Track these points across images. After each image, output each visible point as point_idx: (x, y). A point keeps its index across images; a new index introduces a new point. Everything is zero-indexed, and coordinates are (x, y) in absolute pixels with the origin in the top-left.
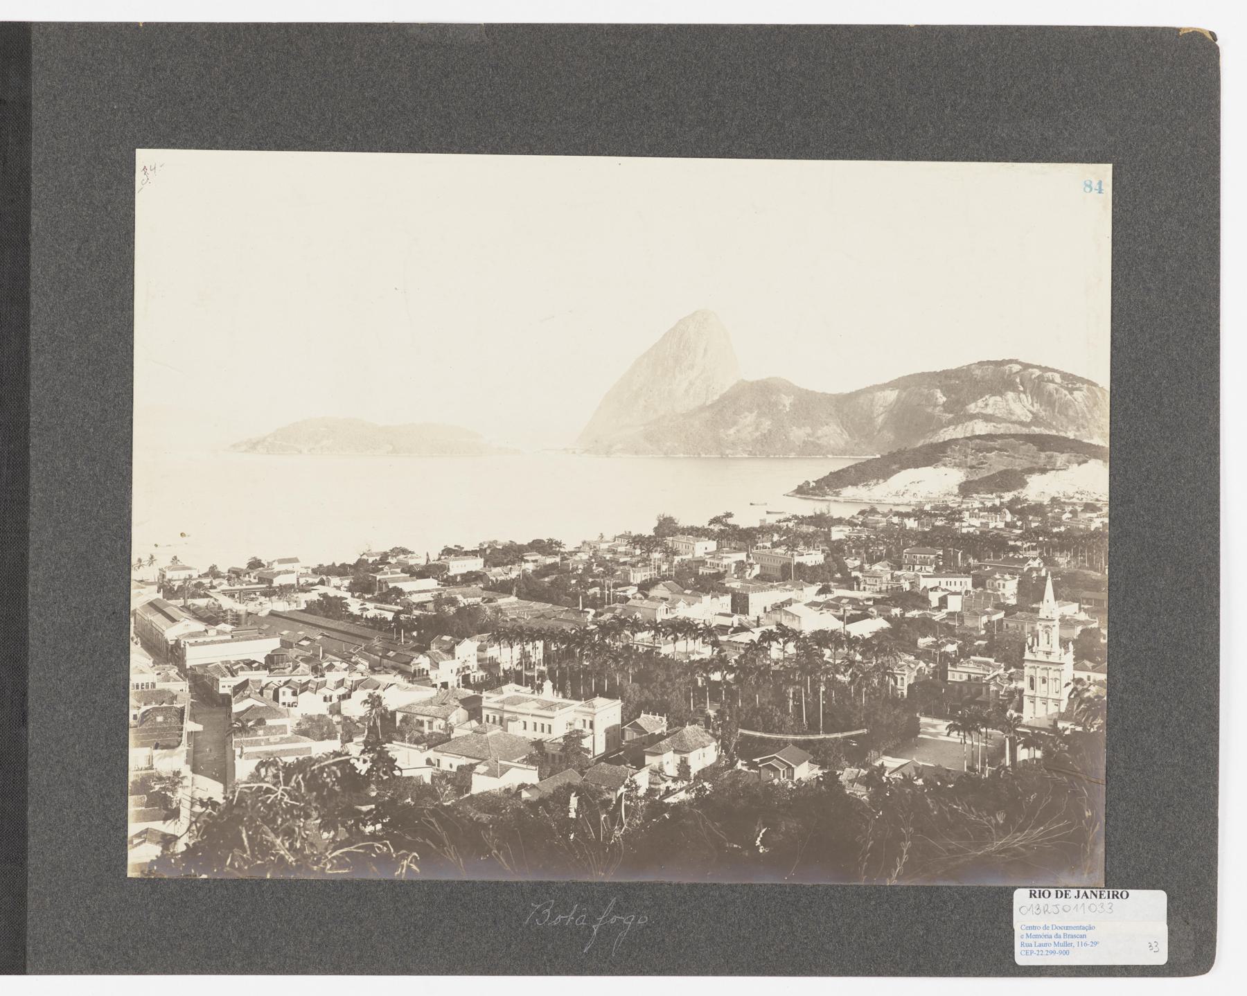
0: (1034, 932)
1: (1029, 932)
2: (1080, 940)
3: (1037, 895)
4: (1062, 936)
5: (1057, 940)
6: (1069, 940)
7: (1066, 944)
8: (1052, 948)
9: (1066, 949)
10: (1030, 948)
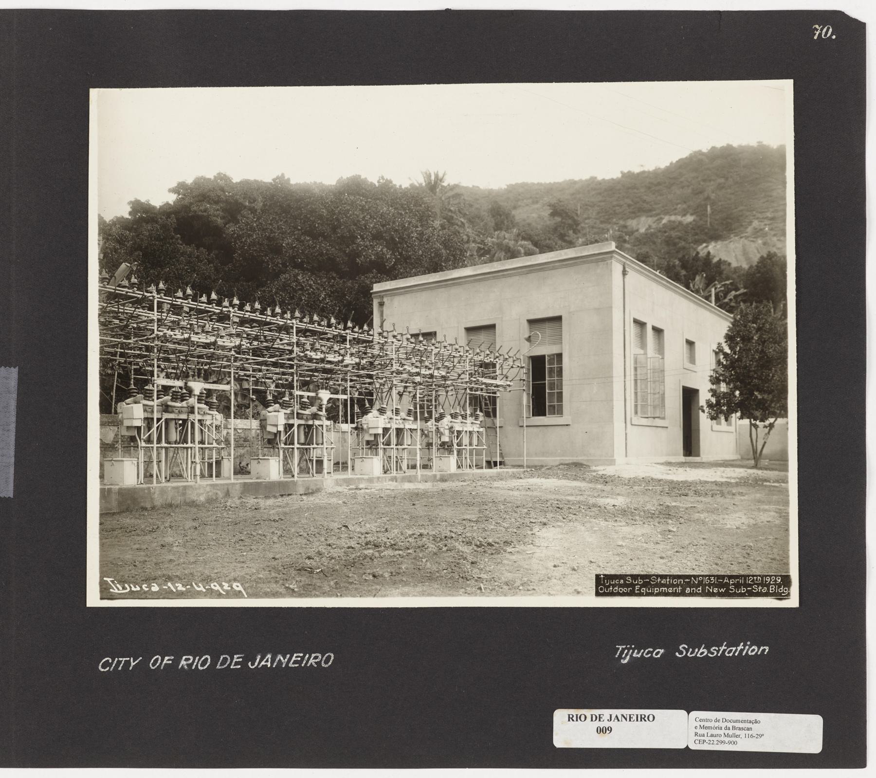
0: (707, 724)
1: (702, 724)
2: (747, 732)
4: (731, 728)
5: (727, 732)
6: (738, 732)
8: (722, 738)
9: (734, 739)
10: (702, 738)
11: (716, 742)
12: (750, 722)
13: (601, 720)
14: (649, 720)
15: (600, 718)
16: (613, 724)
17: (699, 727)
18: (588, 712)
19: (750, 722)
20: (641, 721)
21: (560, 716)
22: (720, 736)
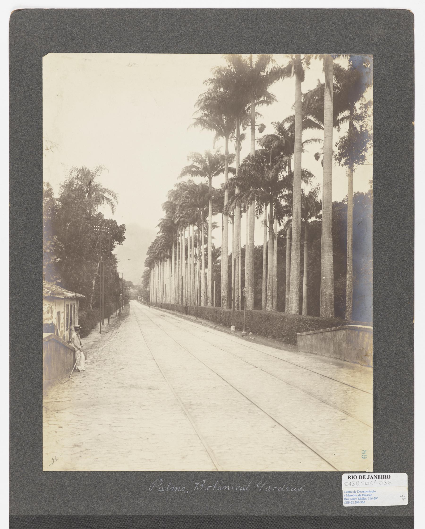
0: (350, 494)
1: (348, 494)
2: (370, 497)
3: (351, 478)
4: (362, 495)
5: (359, 497)
6: (365, 497)
7: (363, 499)
8: (358, 500)
9: (363, 500)
11: (354, 502)
12: (371, 492)
17: (346, 496)
19: (371, 492)
22: (356, 499)
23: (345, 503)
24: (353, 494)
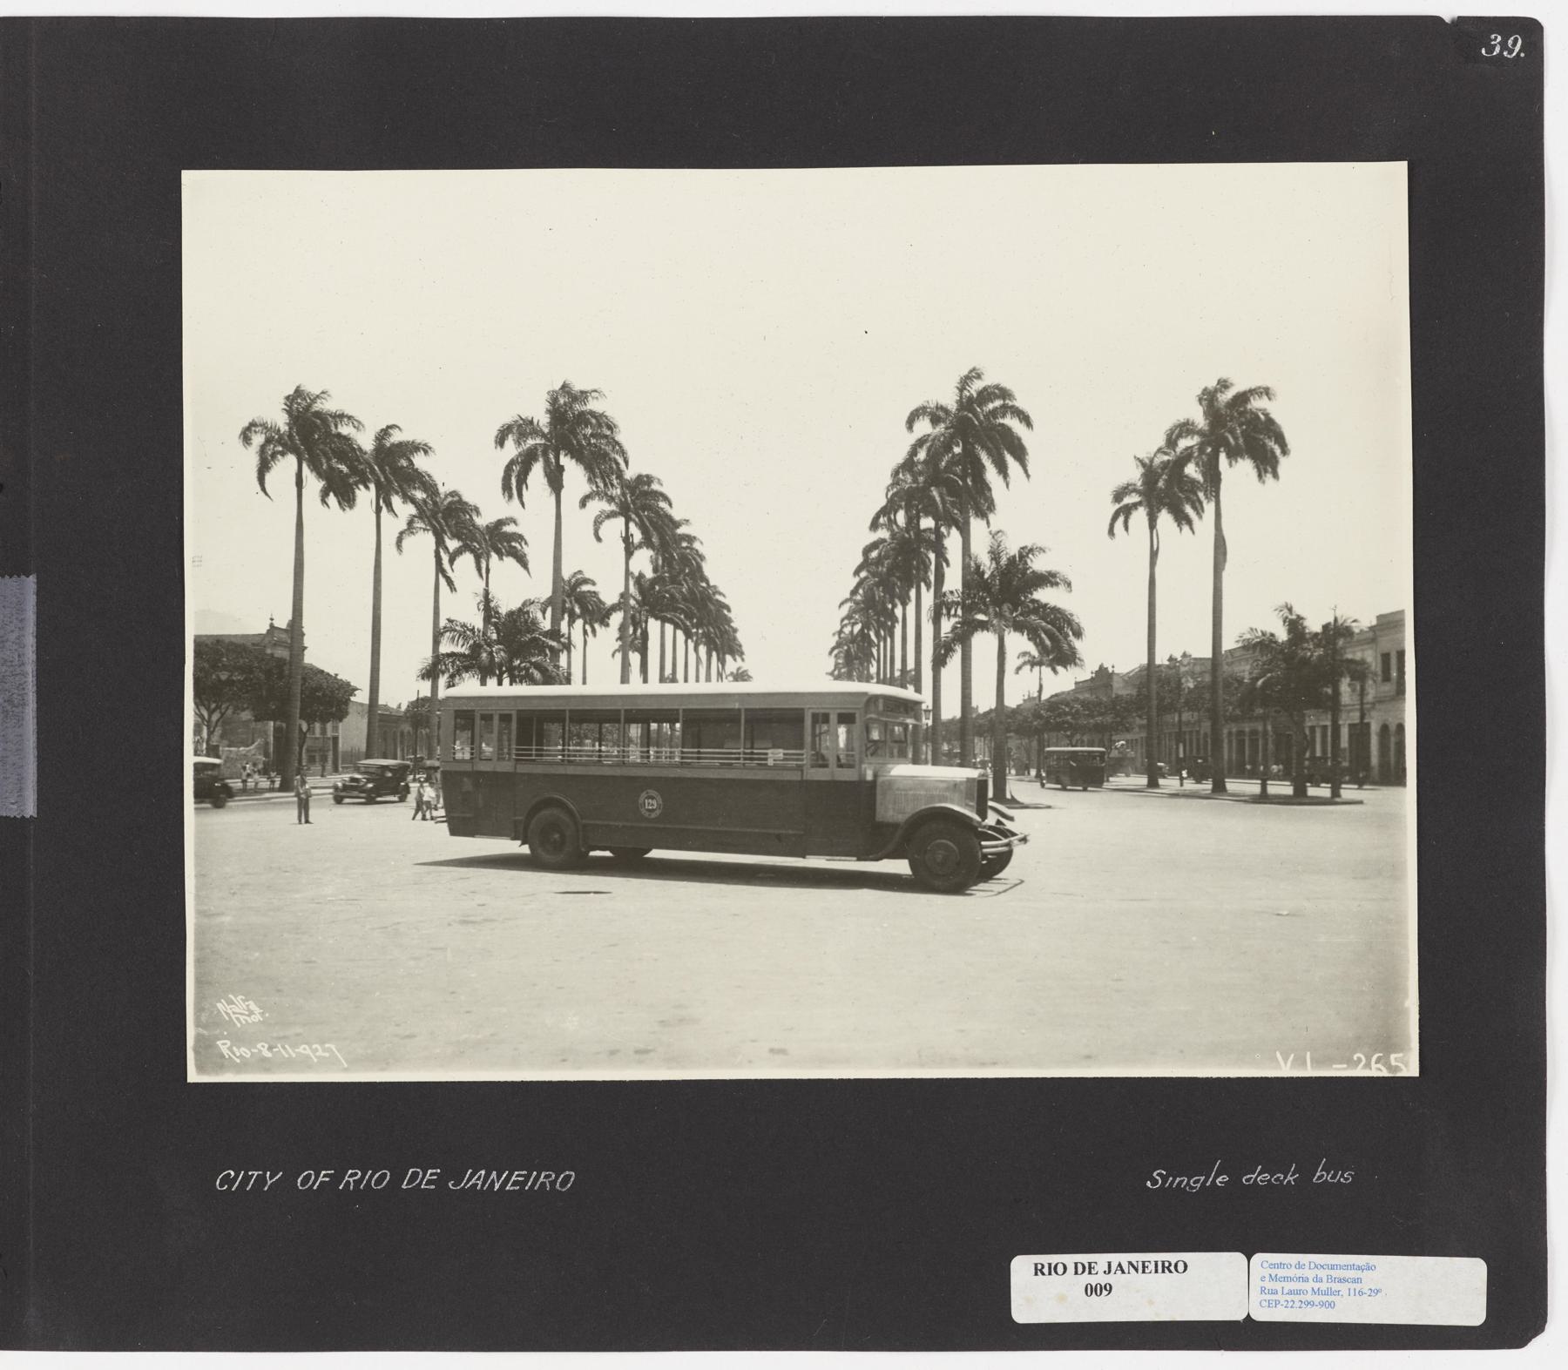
0: (1281, 1273)
1: (1274, 1272)
2: (1355, 1285)
4: (1325, 1279)
5: (1316, 1286)
6: (1336, 1286)
7: (1329, 1292)
8: (1309, 1297)
9: (1330, 1298)
10: (1274, 1297)
11: (1297, 1304)
12: (1359, 1268)
13: (1093, 1272)
14: (1177, 1270)
15: (1090, 1268)
16: (1115, 1279)
17: (1267, 1278)
18: (1069, 1259)
19: (1359, 1268)
20: (1163, 1272)
21: (1021, 1267)
22: (1304, 1292)
23: (1264, 1304)
24: (1292, 1272)
